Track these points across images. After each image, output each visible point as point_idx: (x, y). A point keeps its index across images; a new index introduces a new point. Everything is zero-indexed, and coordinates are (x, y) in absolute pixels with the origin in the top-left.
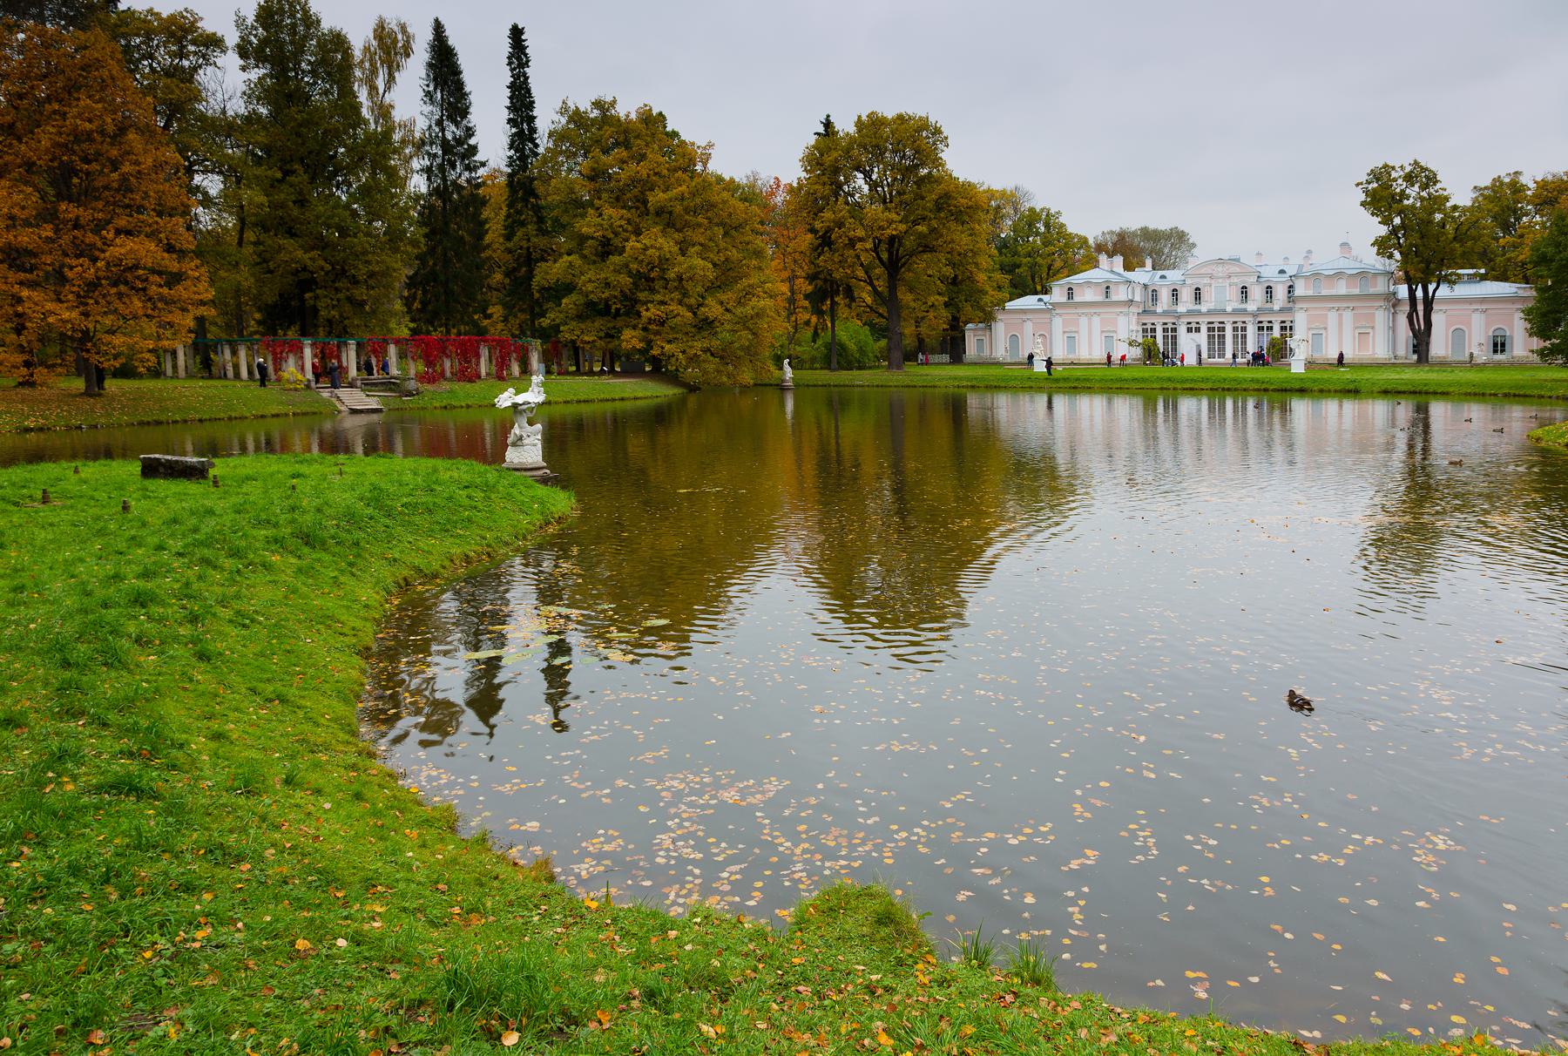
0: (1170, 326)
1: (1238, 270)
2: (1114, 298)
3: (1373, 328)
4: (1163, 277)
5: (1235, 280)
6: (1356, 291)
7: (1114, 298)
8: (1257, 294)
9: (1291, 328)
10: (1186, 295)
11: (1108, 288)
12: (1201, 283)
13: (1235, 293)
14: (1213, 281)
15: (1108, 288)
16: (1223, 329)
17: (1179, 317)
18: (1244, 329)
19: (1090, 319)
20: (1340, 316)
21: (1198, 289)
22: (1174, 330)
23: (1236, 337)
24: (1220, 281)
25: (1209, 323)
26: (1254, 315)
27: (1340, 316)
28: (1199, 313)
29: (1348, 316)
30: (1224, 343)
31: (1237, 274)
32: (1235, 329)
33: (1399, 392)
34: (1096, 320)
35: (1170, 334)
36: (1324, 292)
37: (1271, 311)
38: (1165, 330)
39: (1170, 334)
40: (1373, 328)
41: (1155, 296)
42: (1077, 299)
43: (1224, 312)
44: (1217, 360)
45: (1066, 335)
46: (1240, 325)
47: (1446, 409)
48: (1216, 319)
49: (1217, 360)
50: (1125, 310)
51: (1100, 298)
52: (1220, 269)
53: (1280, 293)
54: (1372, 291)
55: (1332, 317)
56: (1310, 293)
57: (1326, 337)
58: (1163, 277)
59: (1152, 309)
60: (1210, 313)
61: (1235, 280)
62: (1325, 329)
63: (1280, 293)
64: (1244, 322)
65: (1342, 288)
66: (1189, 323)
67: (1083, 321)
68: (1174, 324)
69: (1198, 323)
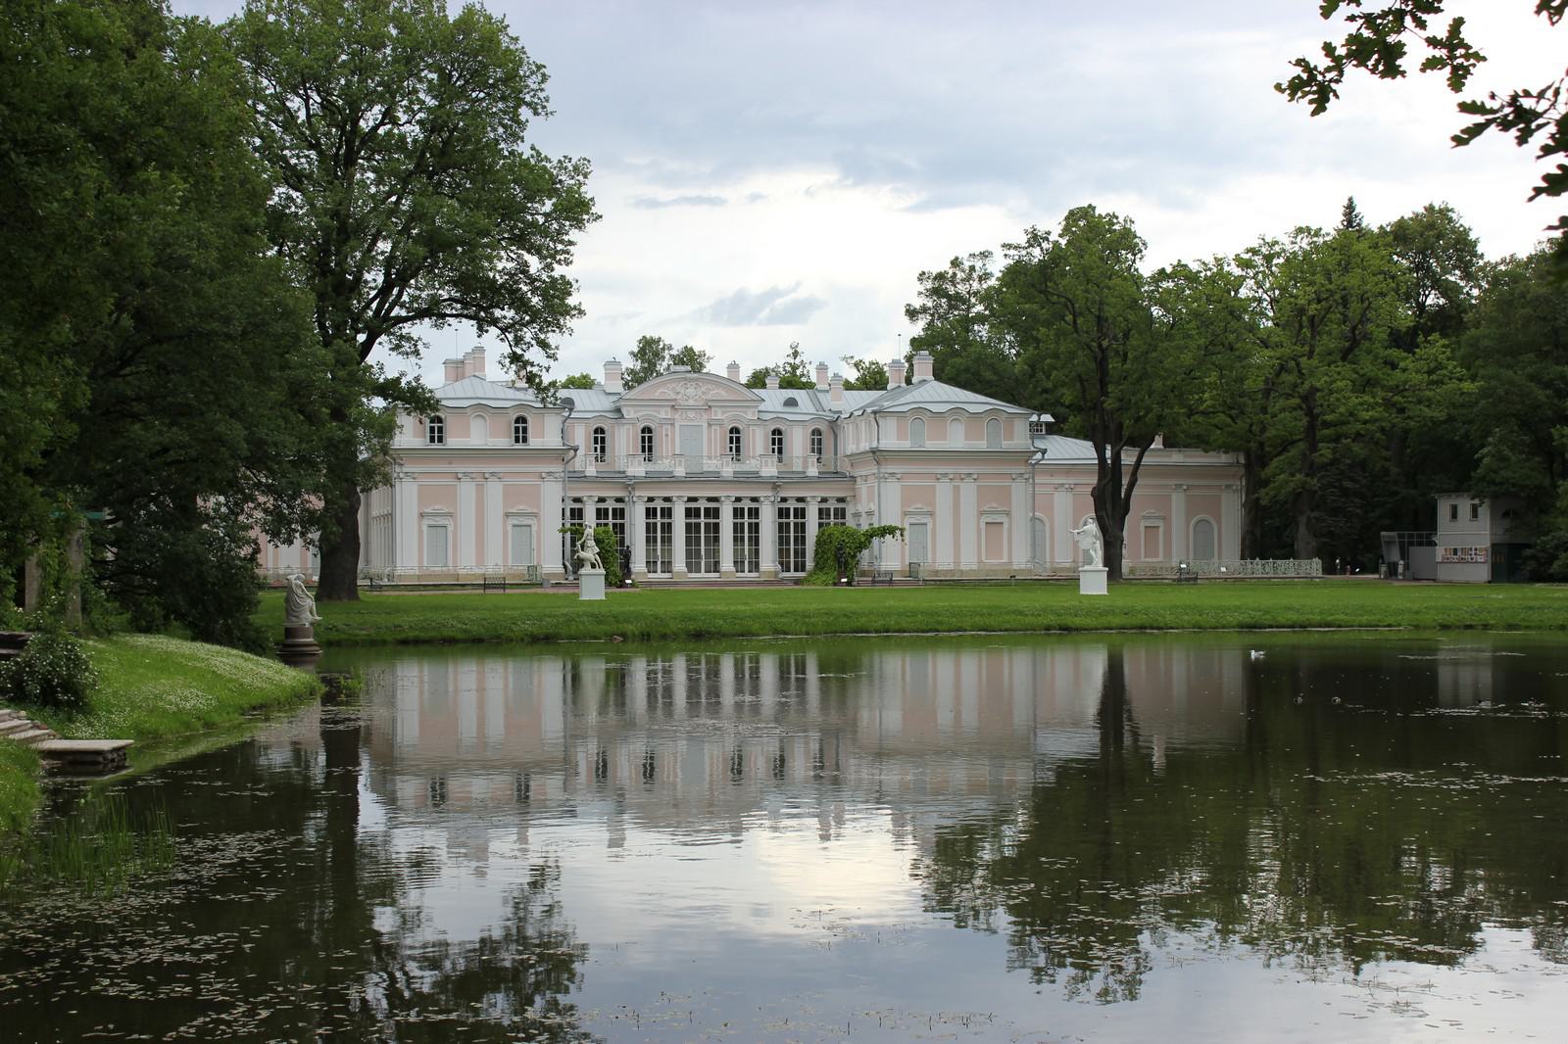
0: (610, 505)
1: (723, 394)
2: (534, 442)
3: (1008, 514)
5: (718, 414)
6: (982, 445)
8: (757, 441)
9: (841, 514)
10: (623, 442)
11: (521, 420)
12: (657, 416)
13: (720, 439)
15: (521, 420)
16: (716, 513)
18: (754, 513)
19: (480, 488)
20: (957, 489)
21: (647, 430)
22: (619, 513)
23: (738, 528)
24: (691, 414)
25: (691, 499)
26: (775, 487)
27: (957, 489)
28: (670, 480)
29: (969, 490)
30: (717, 539)
31: (724, 404)
32: (738, 513)
33: (451, 641)
34: (495, 490)
35: (611, 520)
36: (930, 445)
37: (804, 480)
38: (601, 514)
39: (611, 520)
40: (1008, 514)
42: (452, 441)
43: (715, 479)
44: (703, 575)
45: (426, 522)
46: (746, 505)
47: (980, 661)
48: (659, 493)
49: (703, 575)
50: (557, 468)
51: (504, 442)
52: (691, 391)
53: (798, 443)
54: (1006, 445)
55: (943, 492)
56: (906, 445)
57: (934, 530)
60: (692, 479)
61: (718, 414)
62: (932, 514)
63: (798, 443)
64: (754, 500)
65: (957, 439)
66: (651, 499)
67: (467, 490)
68: (619, 500)
69: (667, 499)
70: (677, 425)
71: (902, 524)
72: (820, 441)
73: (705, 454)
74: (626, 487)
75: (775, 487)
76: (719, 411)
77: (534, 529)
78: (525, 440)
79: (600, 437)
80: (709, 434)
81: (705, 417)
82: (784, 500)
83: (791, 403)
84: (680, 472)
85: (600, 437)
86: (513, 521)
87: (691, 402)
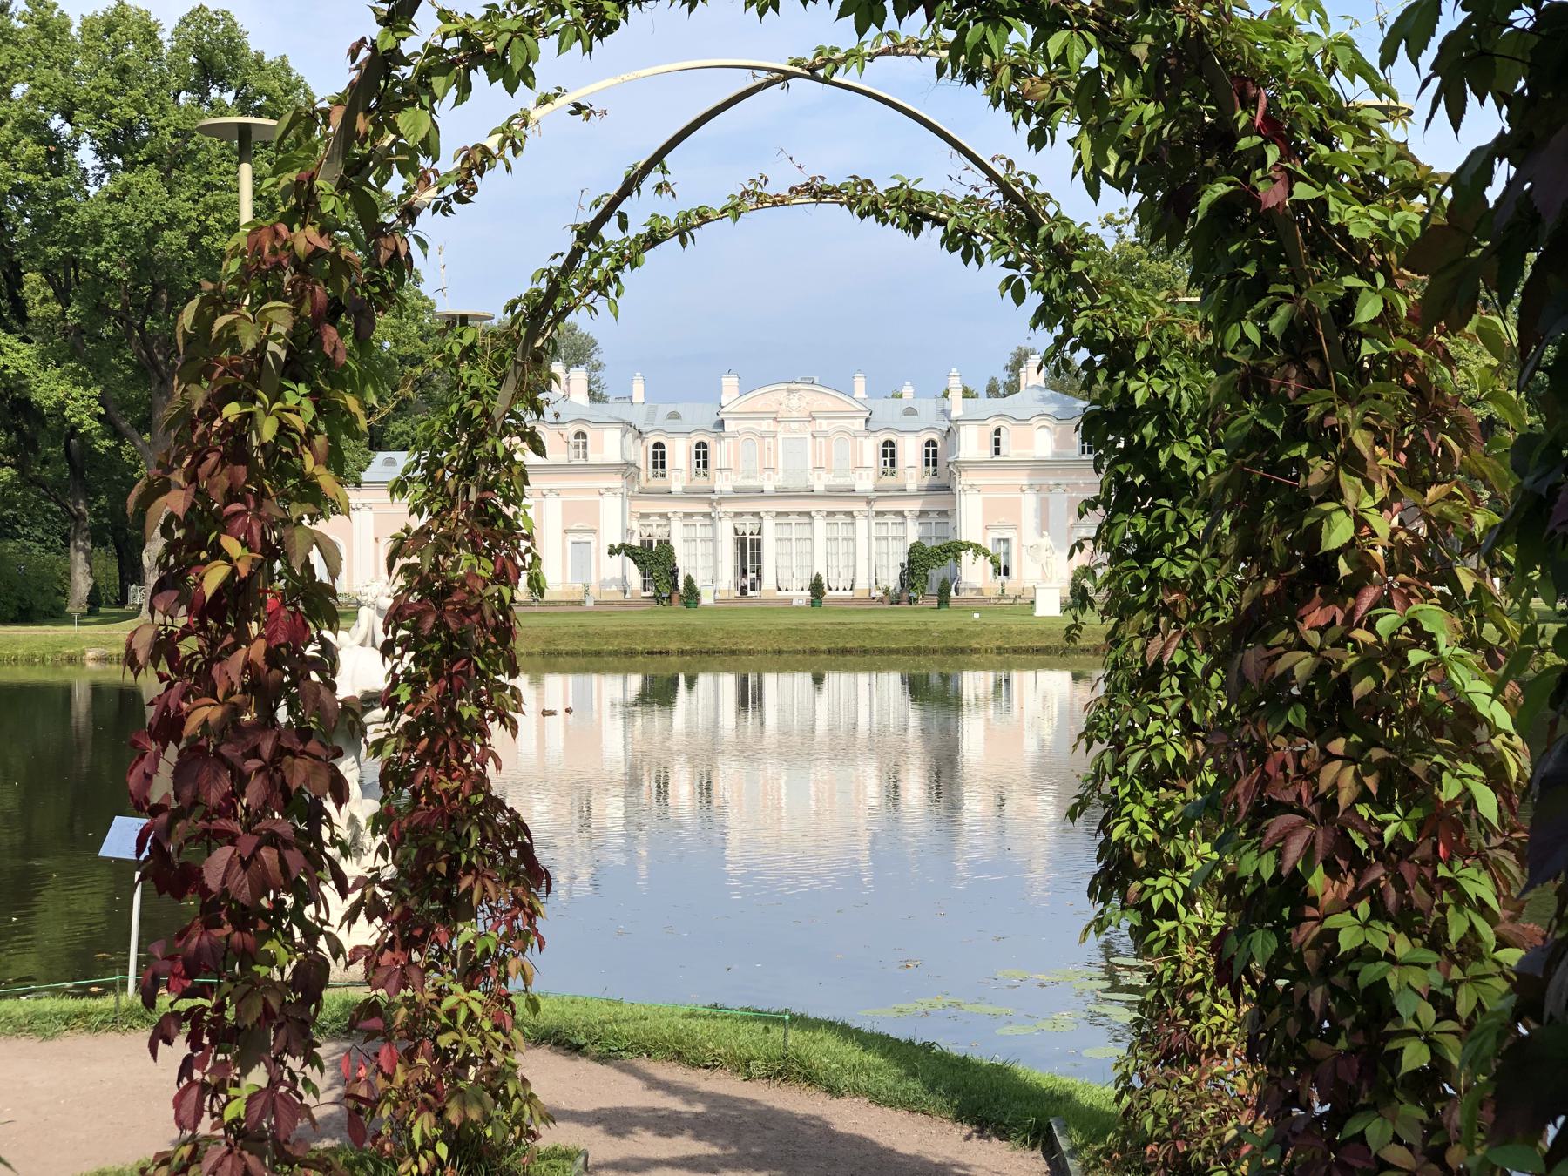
4: (674, 416)
7: (593, 458)
14: (780, 428)
17: (720, 501)
24: (794, 426)
25: (779, 514)
41: (659, 458)
43: (810, 494)
53: (911, 452)
58: (674, 416)
59: (657, 483)
60: (782, 494)
68: (707, 515)
70: (780, 437)
71: (984, 539)
72: (935, 453)
73: (810, 466)
74: (711, 502)
75: (869, 501)
76: (824, 422)
77: (594, 545)
78: (585, 456)
79: (702, 455)
80: (814, 446)
81: (809, 428)
82: (879, 514)
83: (910, 411)
84: (769, 487)
85: (702, 455)
86: (571, 537)
87: (795, 414)
